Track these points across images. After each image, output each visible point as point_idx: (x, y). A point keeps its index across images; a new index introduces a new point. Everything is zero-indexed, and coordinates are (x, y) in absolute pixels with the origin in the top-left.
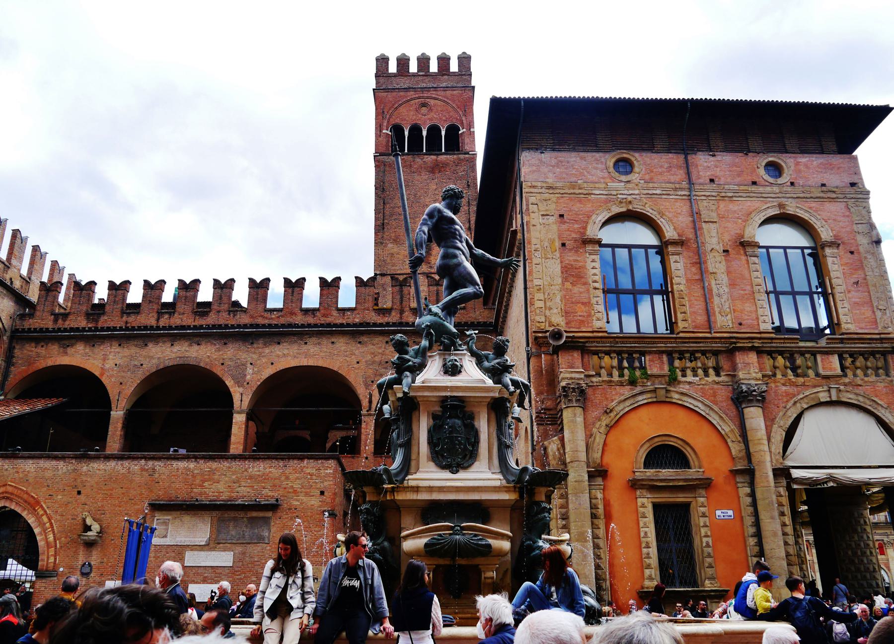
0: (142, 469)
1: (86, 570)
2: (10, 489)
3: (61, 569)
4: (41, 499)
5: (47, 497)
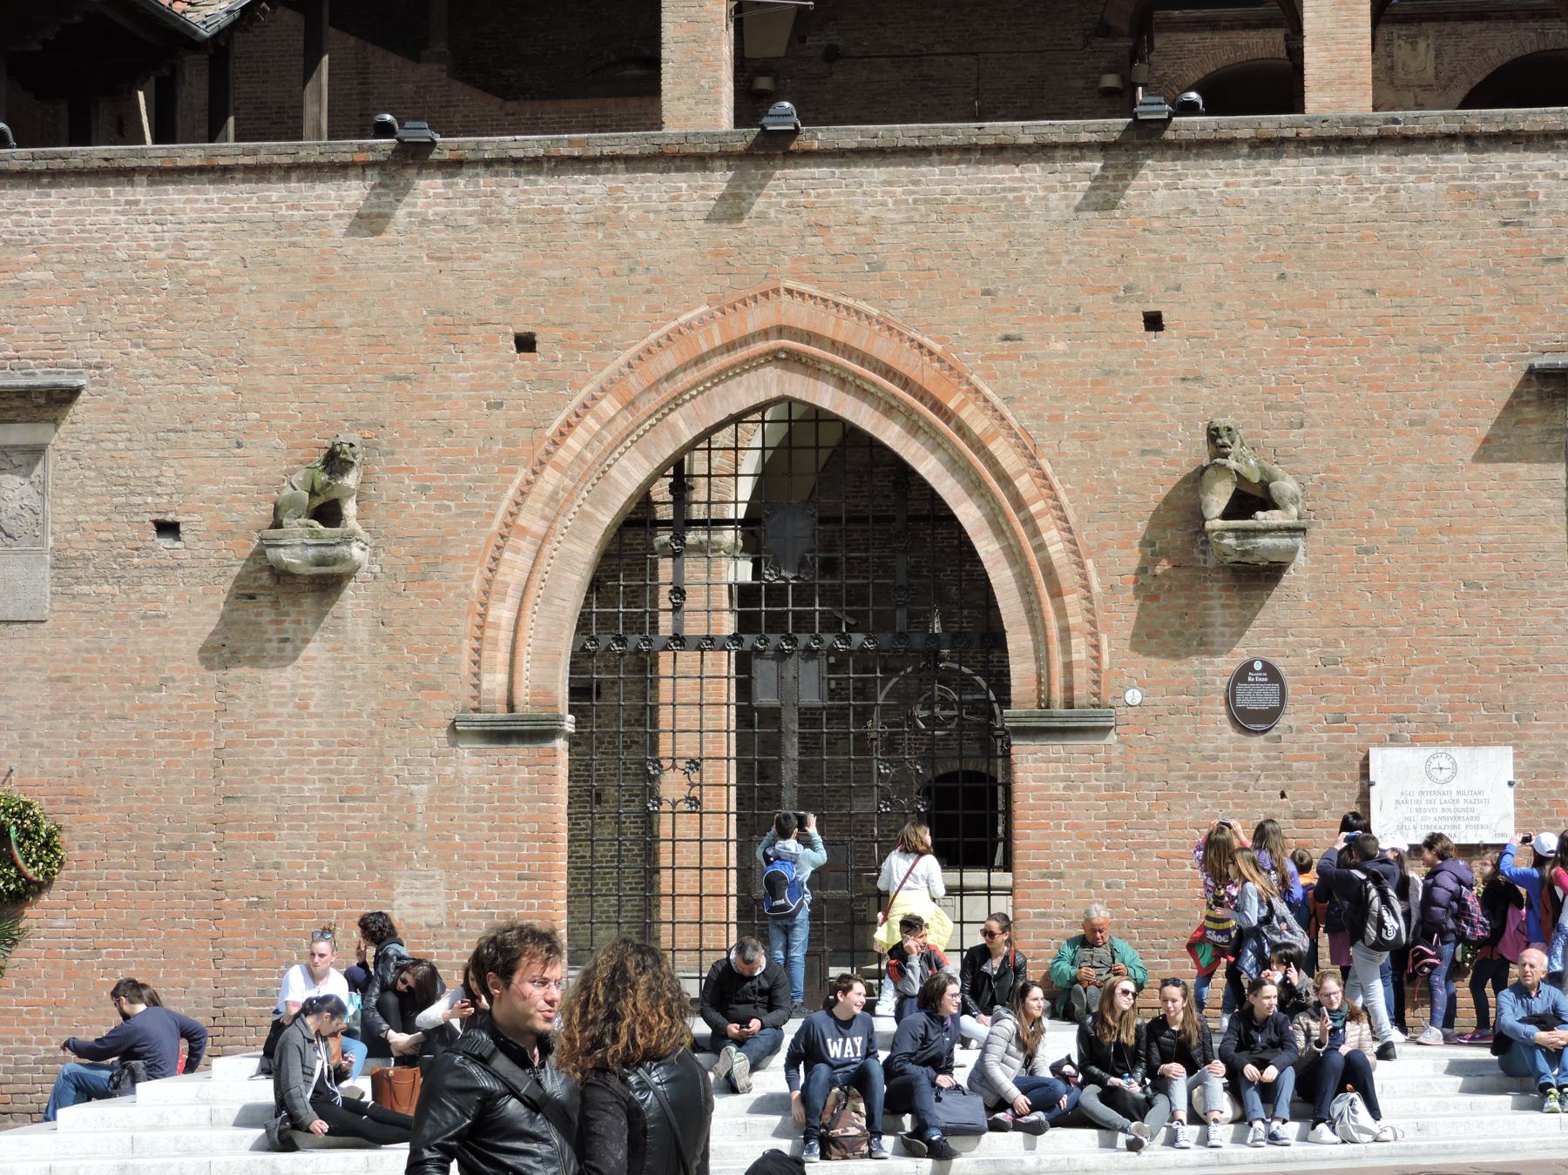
0: (1464, 196)
1: (1257, 697)
2: (798, 314)
3: (1134, 696)
4: (969, 360)
5: (995, 345)
